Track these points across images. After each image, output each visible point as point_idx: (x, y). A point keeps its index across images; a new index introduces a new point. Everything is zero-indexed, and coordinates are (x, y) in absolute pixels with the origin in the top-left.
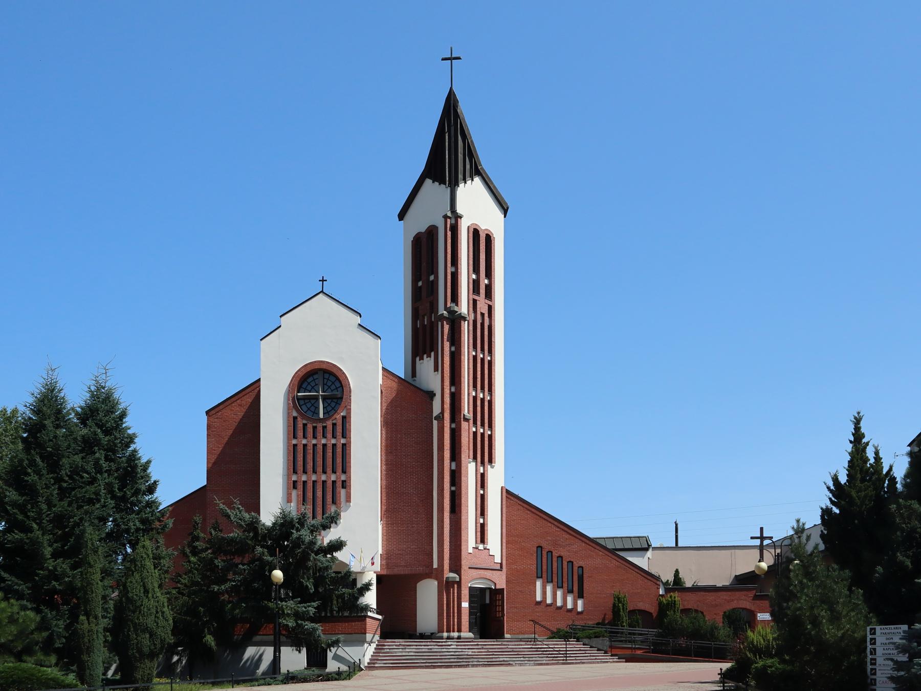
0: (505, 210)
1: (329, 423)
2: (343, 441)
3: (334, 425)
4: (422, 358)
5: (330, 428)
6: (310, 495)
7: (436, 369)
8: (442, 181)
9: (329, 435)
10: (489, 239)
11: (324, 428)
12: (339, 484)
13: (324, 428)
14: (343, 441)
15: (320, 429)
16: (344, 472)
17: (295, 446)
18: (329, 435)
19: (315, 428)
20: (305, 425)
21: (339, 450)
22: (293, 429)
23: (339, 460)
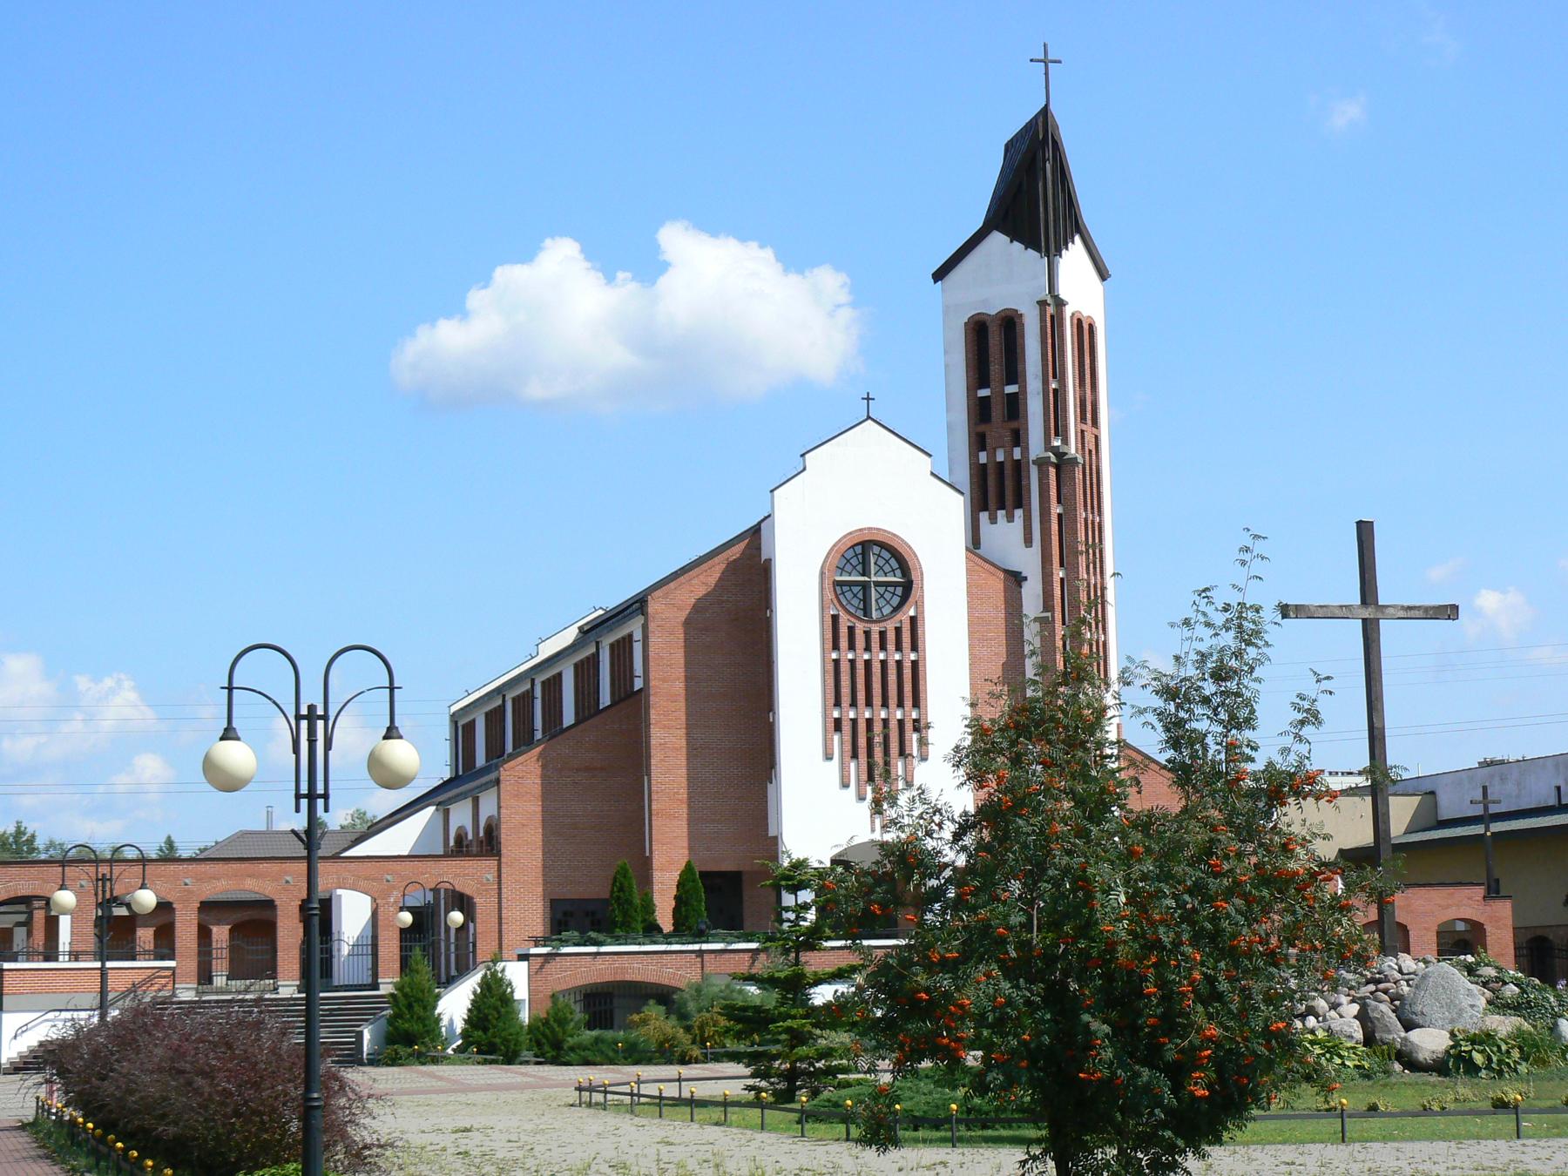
0: (1103, 274)
1: (890, 626)
2: (913, 656)
3: (898, 630)
4: (993, 520)
5: (891, 636)
6: (862, 742)
7: (1028, 541)
8: (1031, 242)
9: (891, 646)
10: (1091, 327)
11: (882, 634)
12: (909, 726)
13: (882, 634)
14: (913, 656)
15: (875, 637)
16: (916, 704)
17: (837, 662)
18: (891, 646)
19: (867, 634)
20: (851, 630)
21: (907, 672)
22: (834, 634)
23: (908, 687)
